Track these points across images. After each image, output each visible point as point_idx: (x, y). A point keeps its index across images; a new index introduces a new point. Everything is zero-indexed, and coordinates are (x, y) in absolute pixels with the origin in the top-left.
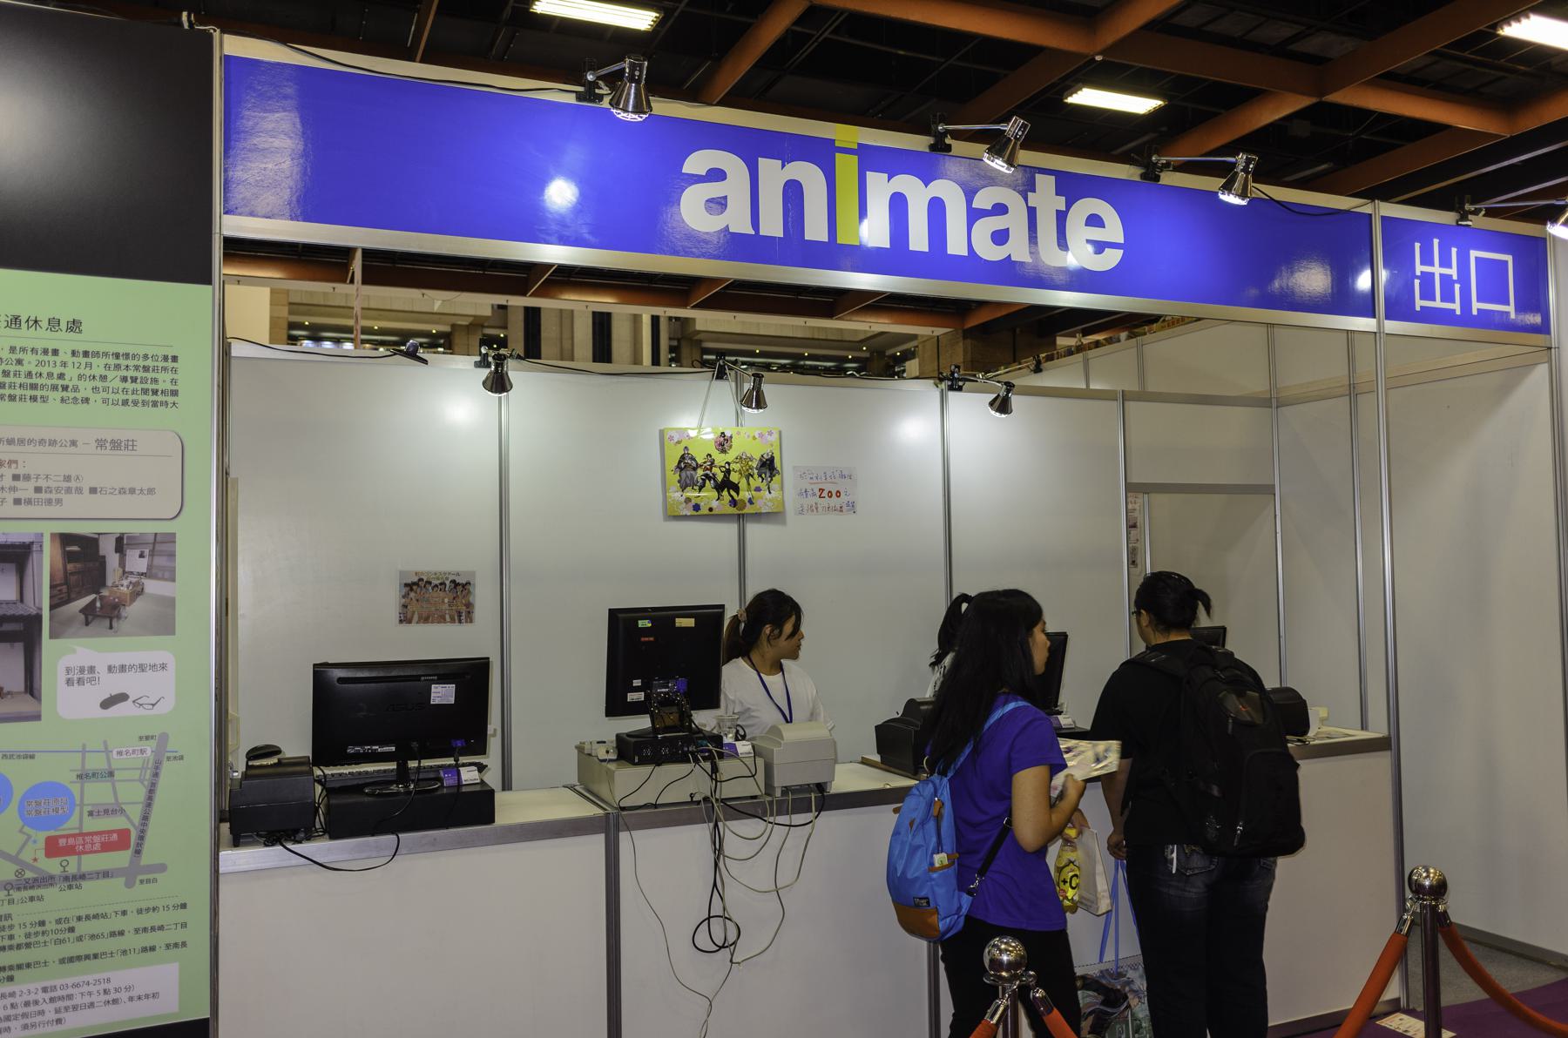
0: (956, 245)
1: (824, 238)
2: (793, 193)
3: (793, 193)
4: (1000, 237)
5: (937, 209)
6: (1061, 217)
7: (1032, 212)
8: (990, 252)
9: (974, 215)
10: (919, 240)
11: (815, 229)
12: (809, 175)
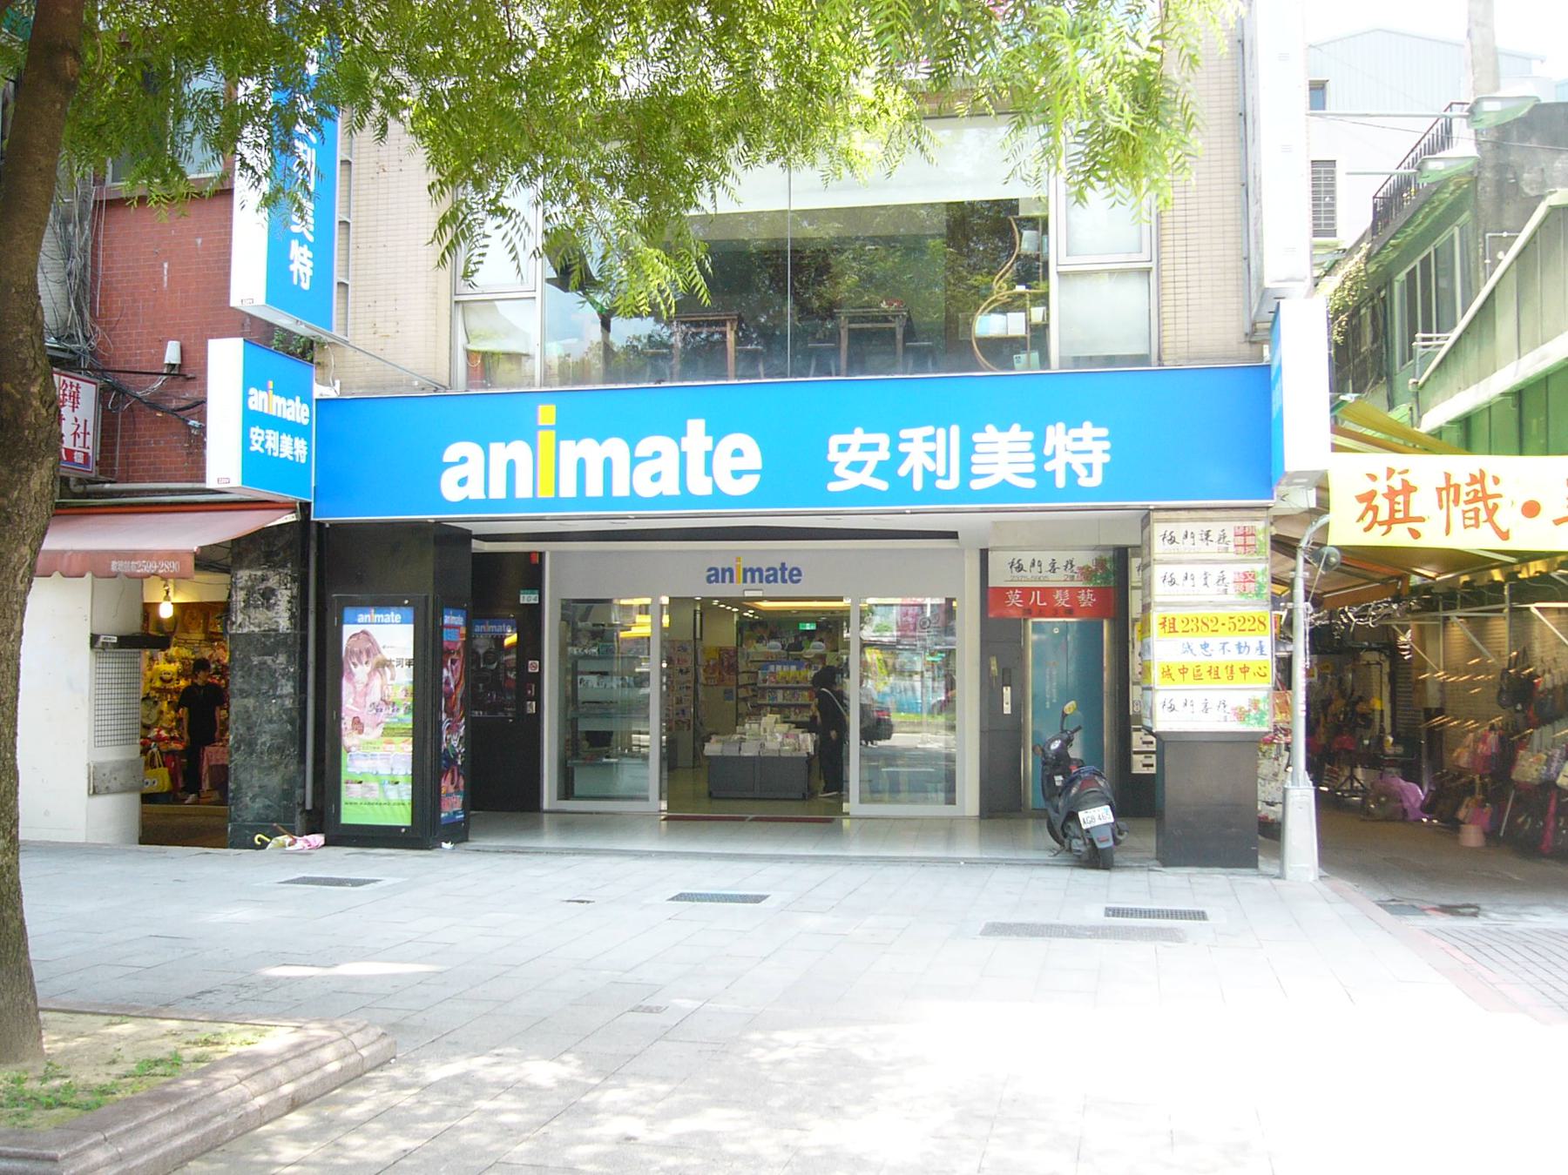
0: (620, 489)
1: (529, 494)
2: (511, 467)
3: (511, 467)
4: (656, 477)
5: (608, 464)
6: (709, 456)
7: (683, 457)
8: (647, 490)
9: (635, 461)
10: (594, 489)
11: (523, 490)
12: (519, 451)
